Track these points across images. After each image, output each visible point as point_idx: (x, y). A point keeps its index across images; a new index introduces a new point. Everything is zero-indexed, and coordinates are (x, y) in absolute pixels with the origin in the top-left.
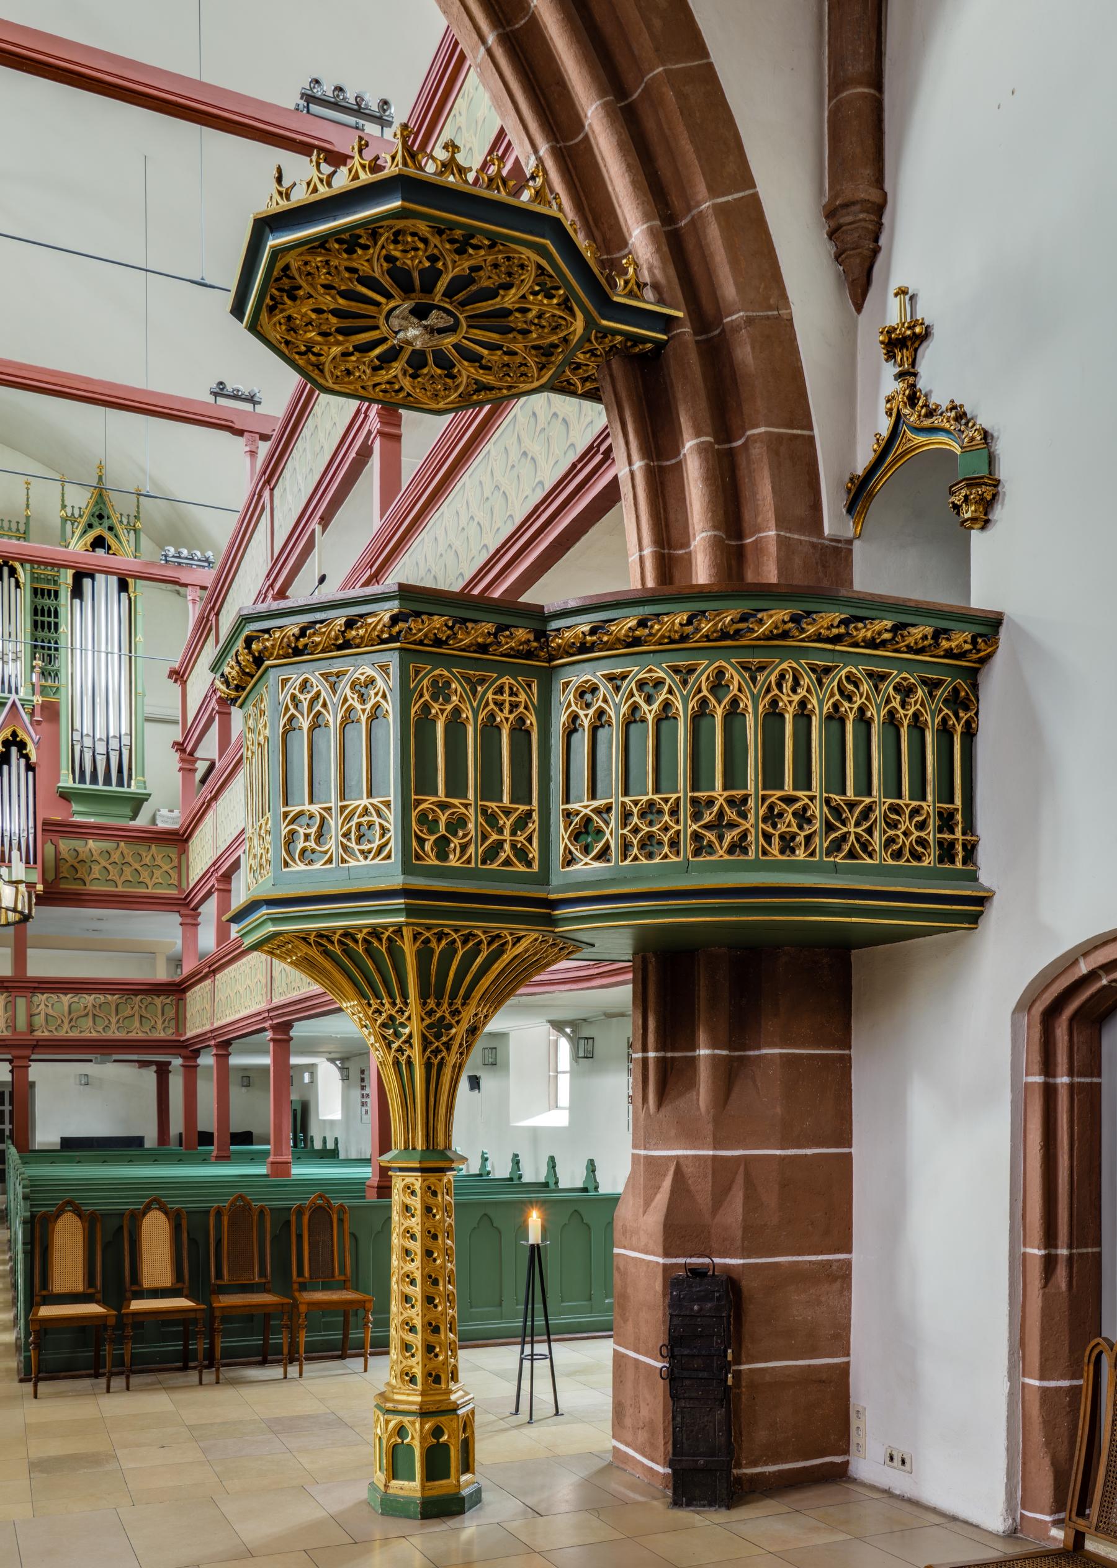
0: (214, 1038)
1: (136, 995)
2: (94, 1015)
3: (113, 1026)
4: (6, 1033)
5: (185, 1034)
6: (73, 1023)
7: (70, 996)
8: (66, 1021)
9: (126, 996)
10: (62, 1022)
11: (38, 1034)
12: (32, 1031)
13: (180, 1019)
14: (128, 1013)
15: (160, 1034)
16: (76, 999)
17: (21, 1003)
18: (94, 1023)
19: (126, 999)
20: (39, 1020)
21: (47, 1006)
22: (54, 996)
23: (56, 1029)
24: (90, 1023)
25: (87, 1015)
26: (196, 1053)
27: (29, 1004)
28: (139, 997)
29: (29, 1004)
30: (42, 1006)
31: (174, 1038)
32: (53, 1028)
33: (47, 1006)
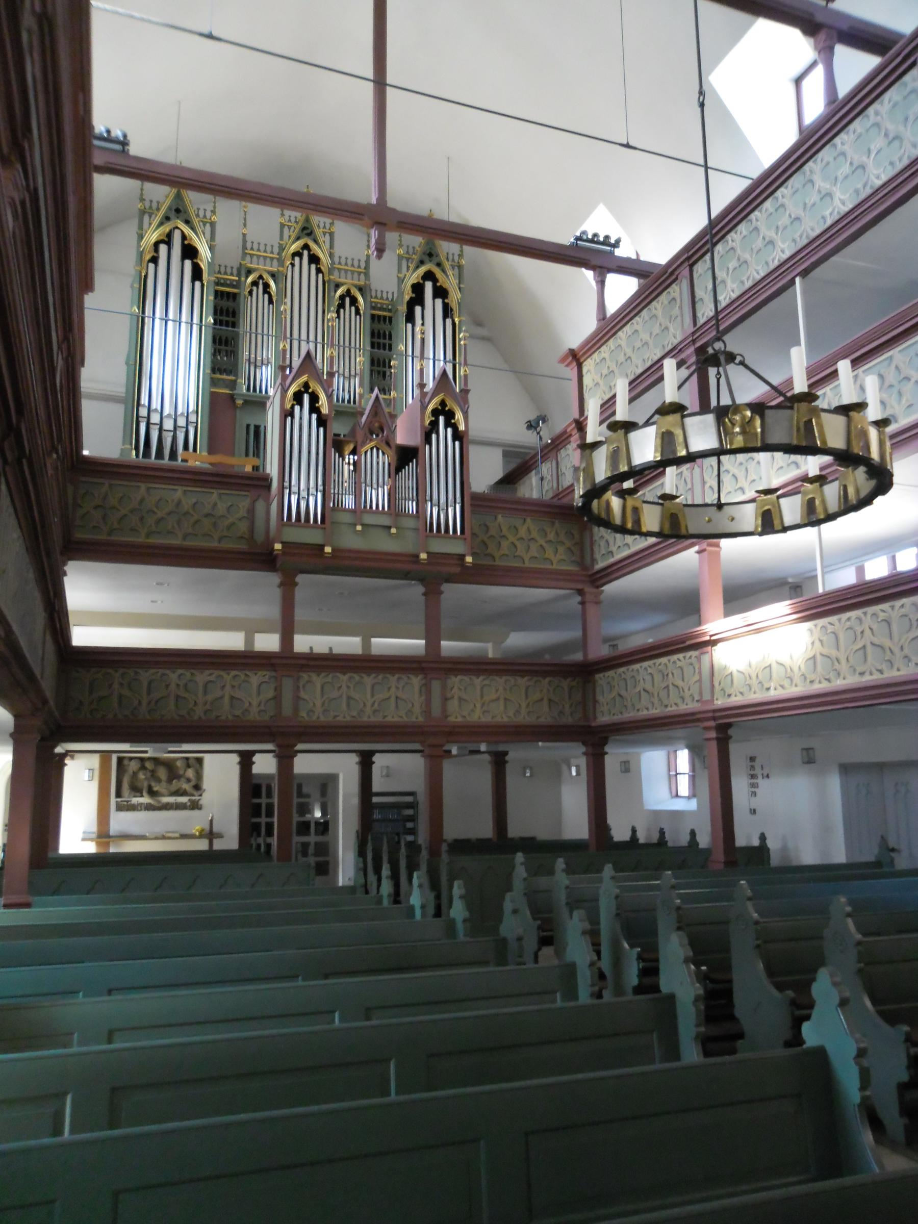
0: (714, 719)
1: (544, 678)
2: (505, 699)
3: (524, 711)
4: (421, 719)
5: (595, 718)
6: (485, 708)
7: (481, 678)
8: (478, 706)
9: (535, 679)
10: (475, 706)
11: (452, 719)
12: (446, 717)
13: (588, 702)
14: (537, 696)
15: (568, 720)
16: (487, 682)
17: (436, 685)
18: (505, 707)
19: (535, 682)
20: (453, 705)
21: (460, 689)
22: (466, 679)
23: (469, 715)
24: (502, 708)
25: (498, 699)
26: (604, 741)
27: (444, 687)
28: (548, 679)
29: (444, 687)
30: (455, 690)
31: (582, 723)
32: (465, 713)
33: (460, 689)
